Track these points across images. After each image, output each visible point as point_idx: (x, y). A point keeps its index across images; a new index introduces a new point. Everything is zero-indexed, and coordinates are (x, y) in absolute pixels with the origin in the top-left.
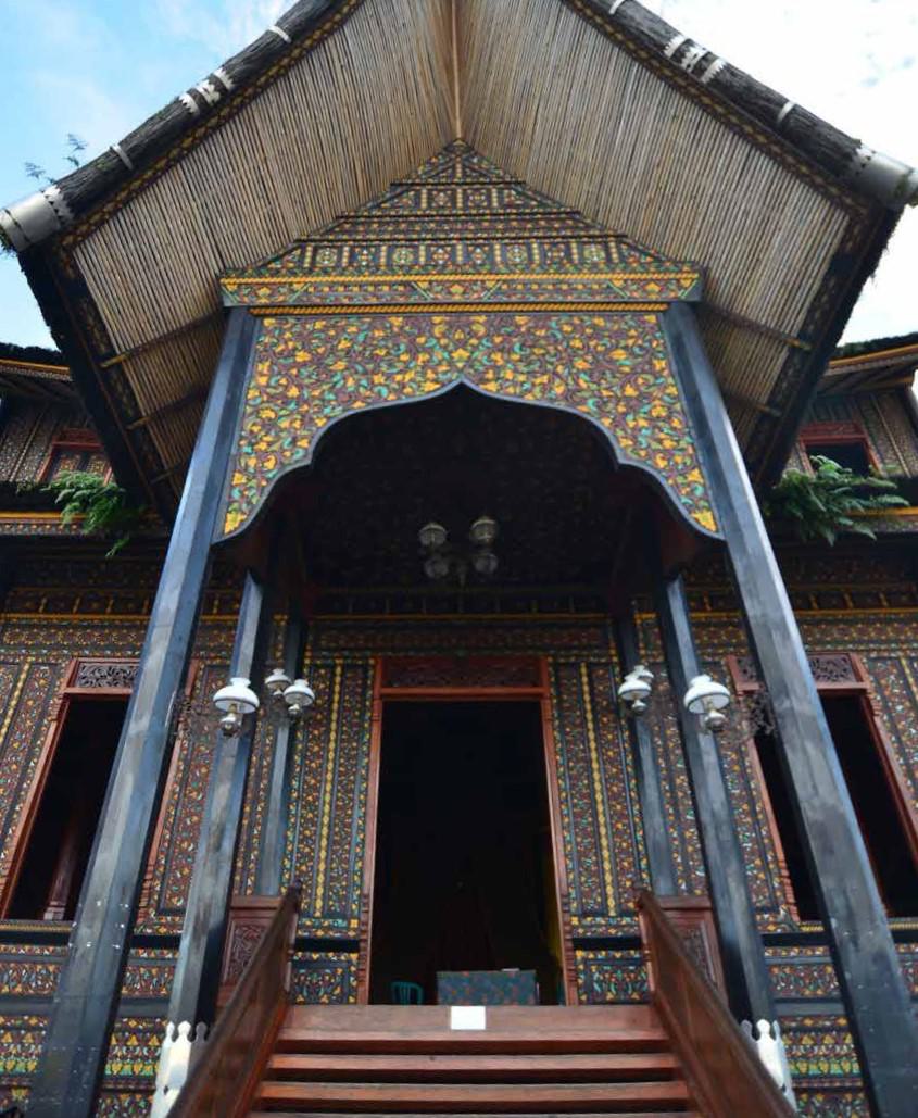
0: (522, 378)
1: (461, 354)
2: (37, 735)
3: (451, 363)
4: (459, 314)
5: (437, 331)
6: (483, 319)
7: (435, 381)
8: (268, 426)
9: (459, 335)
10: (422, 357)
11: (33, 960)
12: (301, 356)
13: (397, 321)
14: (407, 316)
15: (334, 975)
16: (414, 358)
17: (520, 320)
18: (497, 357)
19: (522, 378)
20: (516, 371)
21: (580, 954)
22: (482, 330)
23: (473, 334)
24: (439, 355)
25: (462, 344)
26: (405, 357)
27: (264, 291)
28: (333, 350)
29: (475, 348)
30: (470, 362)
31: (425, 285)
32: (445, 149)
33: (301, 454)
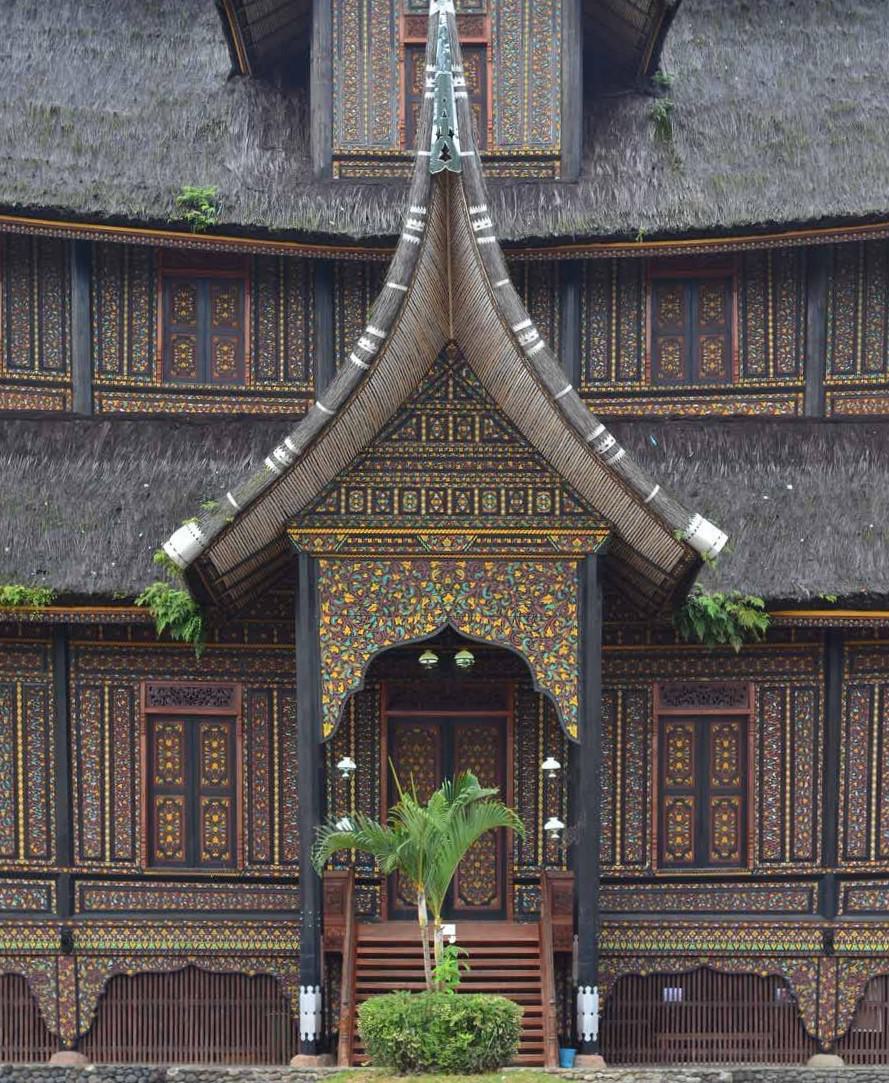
0: (485, 621)
1: (449, 598)
2: (133, 745)
3: (442, 605)
4: (448, 560)
5: (435, 574)
6: (463, 564)
7: (433, 623)
8: (336, 657)
9: (448, 581)
10: (425, 601)
11: (180, 891)
12: (349, 598)
13: (407, 565)
14: (413, 560)
15: (366, 898)
16: (419, 602)
17: (488, 566)
18: (471, 601)
19: (485, 621)
20: (483, 615)
21: (517, 887)
22: (461, 573)
23: (456, 579)
24: (436, 598)
25: (449, 588)
26: (413, 601)
27: (318, 541)
28: (367, 593)
29: (458, 591)
30: (455, 604)
31: (425, 538)
32: (440, 356)
33: (356, 681)
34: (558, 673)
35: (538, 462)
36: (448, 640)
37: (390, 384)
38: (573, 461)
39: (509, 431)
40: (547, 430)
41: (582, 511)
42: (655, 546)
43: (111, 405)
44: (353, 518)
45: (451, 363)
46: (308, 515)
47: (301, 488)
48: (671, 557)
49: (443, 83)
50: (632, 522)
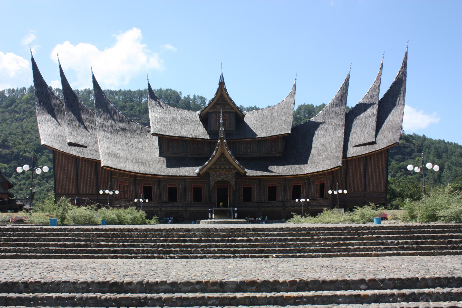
34: (233, 183)
35: (231, 164)
36: (222, 179)
37: (217, 156)
38: (234, 163)
39: (228, 160)
40: (231, 160)
41: (235, 168)
42: (242, 171)
43: (188, 156)
44: (213, 169)
45: (222, 155)
46: (209, 169)
47: (209, 166)
48: (244, 172)
49: (222, 128)
50: (240, 169)
